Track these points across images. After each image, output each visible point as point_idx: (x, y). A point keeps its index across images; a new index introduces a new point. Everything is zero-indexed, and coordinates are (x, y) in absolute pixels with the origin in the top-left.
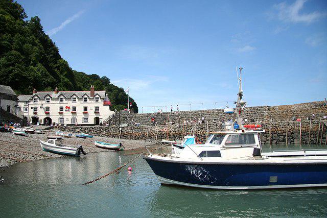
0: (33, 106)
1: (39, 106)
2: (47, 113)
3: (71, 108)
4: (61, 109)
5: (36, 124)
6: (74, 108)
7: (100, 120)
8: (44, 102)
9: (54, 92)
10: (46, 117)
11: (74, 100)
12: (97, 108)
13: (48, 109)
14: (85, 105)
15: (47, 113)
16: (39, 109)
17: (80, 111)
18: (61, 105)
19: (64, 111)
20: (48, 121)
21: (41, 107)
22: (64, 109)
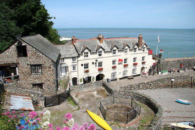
0: (84, 62)
1: (90, 62)
2: (100, 70)
3: (123, 60)
8: (96, 56)
10: (99, 74)
13: (100, 64)
15: (100, 70)
17: (130, 62)
18: (114, 58)
21: (93, 63)
22: (117, 62)
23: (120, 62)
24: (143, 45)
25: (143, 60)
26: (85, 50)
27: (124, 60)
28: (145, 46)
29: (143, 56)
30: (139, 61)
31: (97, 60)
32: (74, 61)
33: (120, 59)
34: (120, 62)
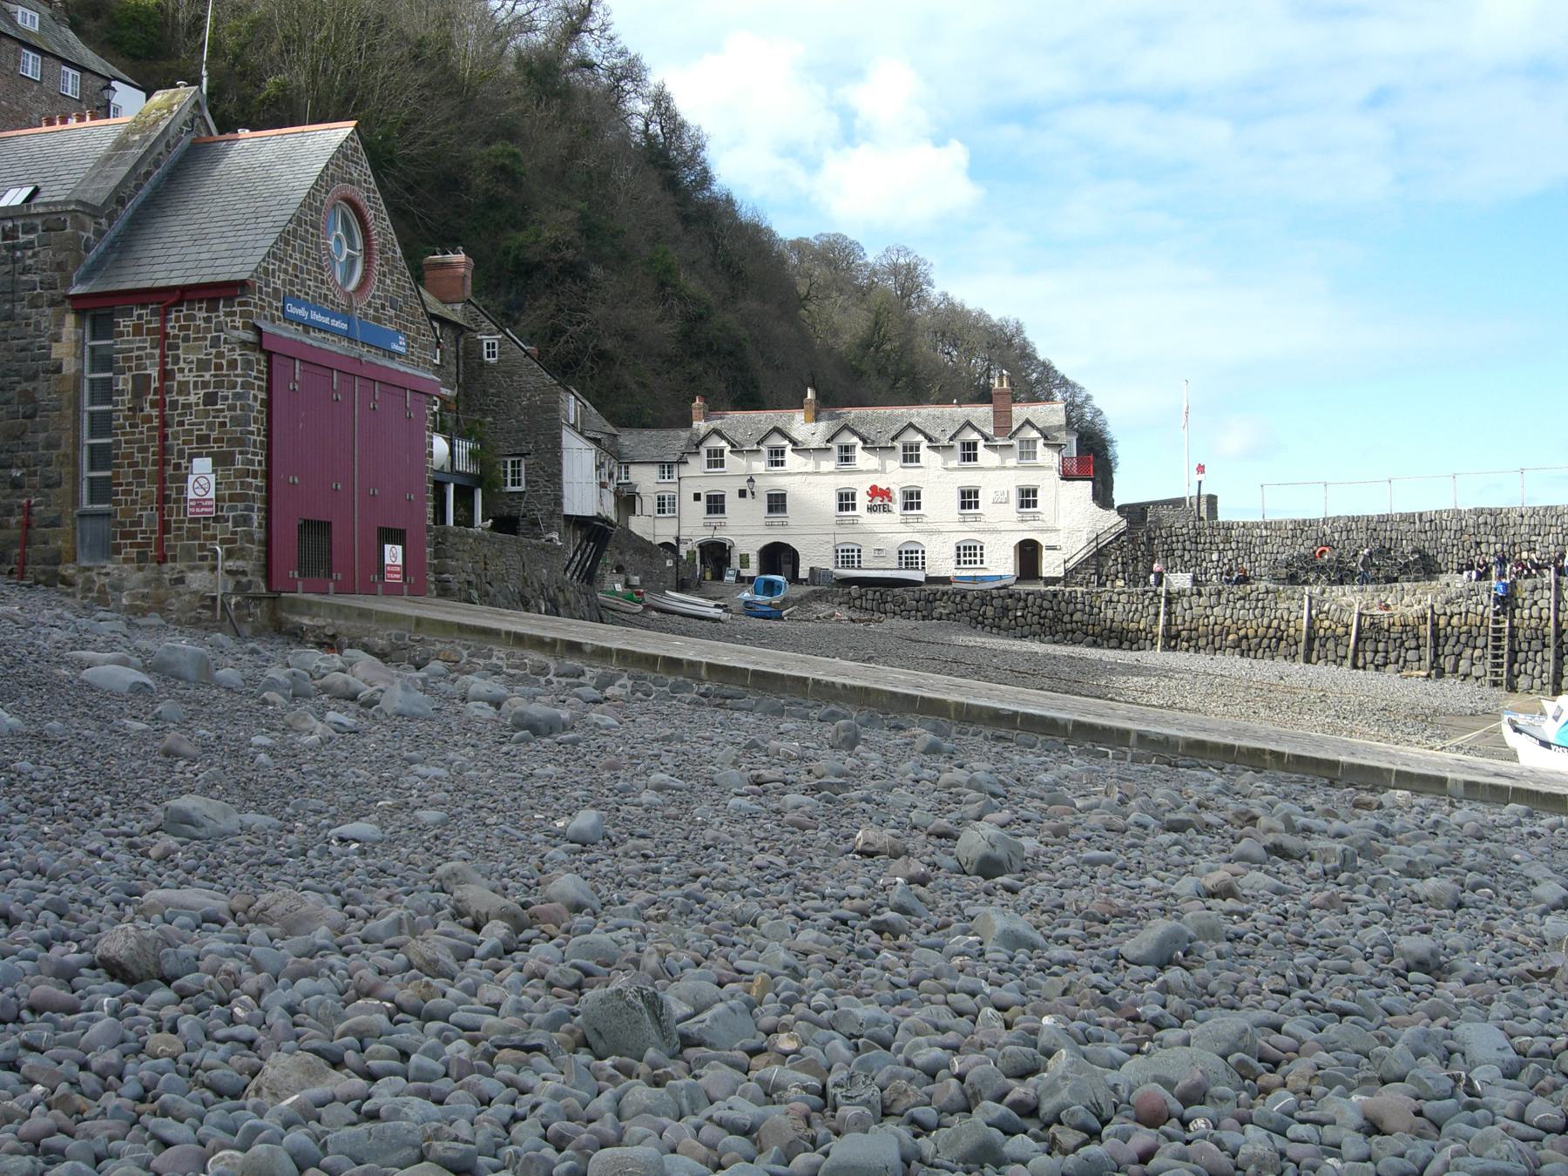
1: (730, 489)
3: (898, 496)
5: (719, 576)
7: (1045, 553)
8: (759, 465)
9: (799, 416)
11: (911, 455)
14: (969, 479)
16: (731, 502)
18: (845, 482)
20: (778, 557)
21: (742, 494)
22: (862, 500)
23: (878, 501)
32: (666, 480)
33: (874, 488)
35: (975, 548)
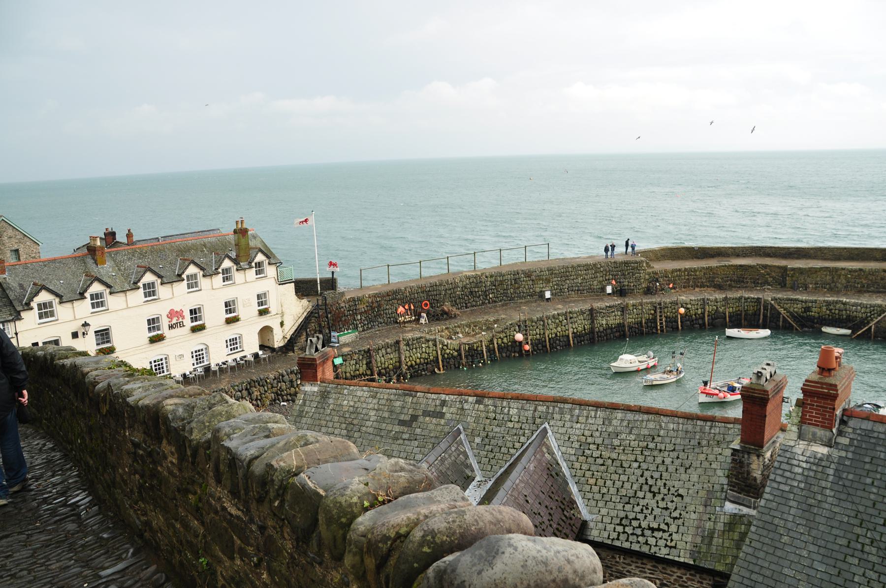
4: (153, 323)
6: (195, 313)
8: (84, 307)
12: (261, 299)
17: (214, 316)
19: (165, 330)
22: (165, 323)
24: (252, 253)
25: (260, 304)
26: (36, 294)
27: (191, 311)
28: (260, 257)
29: (260, 292)
30: (247, 310)
31: (86, 325)
34: (174, 321)
35: (236, 338)
